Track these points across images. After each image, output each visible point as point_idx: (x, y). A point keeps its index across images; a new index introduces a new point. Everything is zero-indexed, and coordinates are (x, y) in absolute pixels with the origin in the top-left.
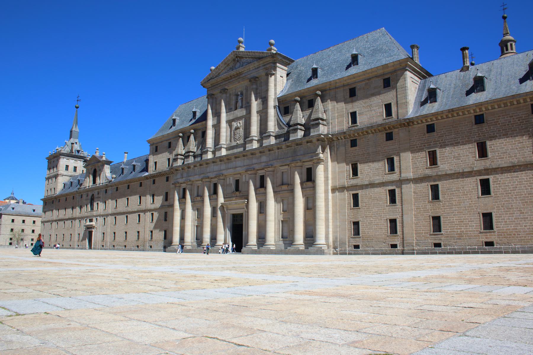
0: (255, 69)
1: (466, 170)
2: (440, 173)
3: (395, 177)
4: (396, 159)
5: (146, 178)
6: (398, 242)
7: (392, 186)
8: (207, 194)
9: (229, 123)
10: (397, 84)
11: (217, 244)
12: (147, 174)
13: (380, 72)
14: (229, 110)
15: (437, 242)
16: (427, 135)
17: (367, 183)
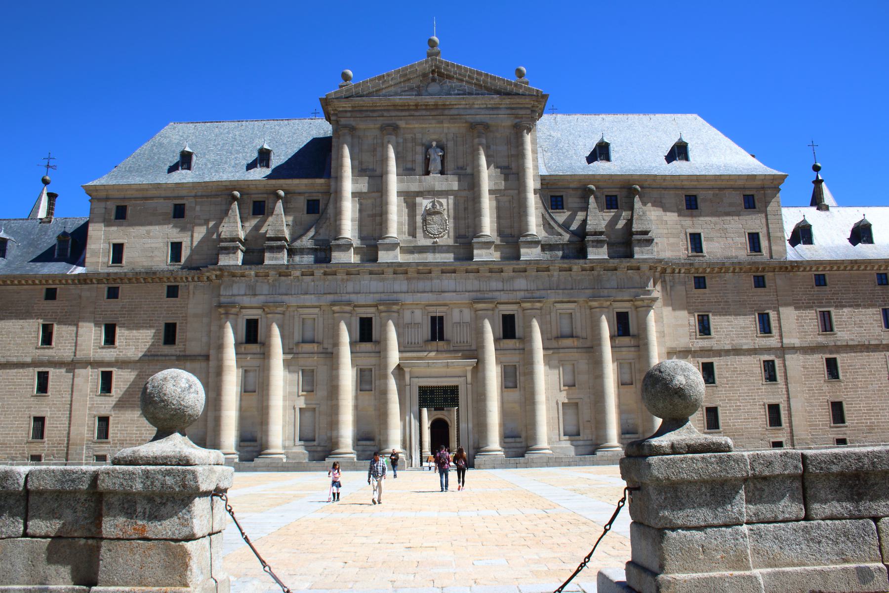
0: (487, 108)
1: (872, 342)
2: (839, 343)
3: (772, 341)
4: (773, 315)
5: (82, 280)
6: (782, 437)
7: (769, 354)
8: (345, 338)
9: (409, 198)
10: (766, 207)
11: (488, 448)
12: (79, 270)
13: (740, 183)
14: (405, 170)
15: (841, 437)
16: (816, 288)
17: (728, 347)
